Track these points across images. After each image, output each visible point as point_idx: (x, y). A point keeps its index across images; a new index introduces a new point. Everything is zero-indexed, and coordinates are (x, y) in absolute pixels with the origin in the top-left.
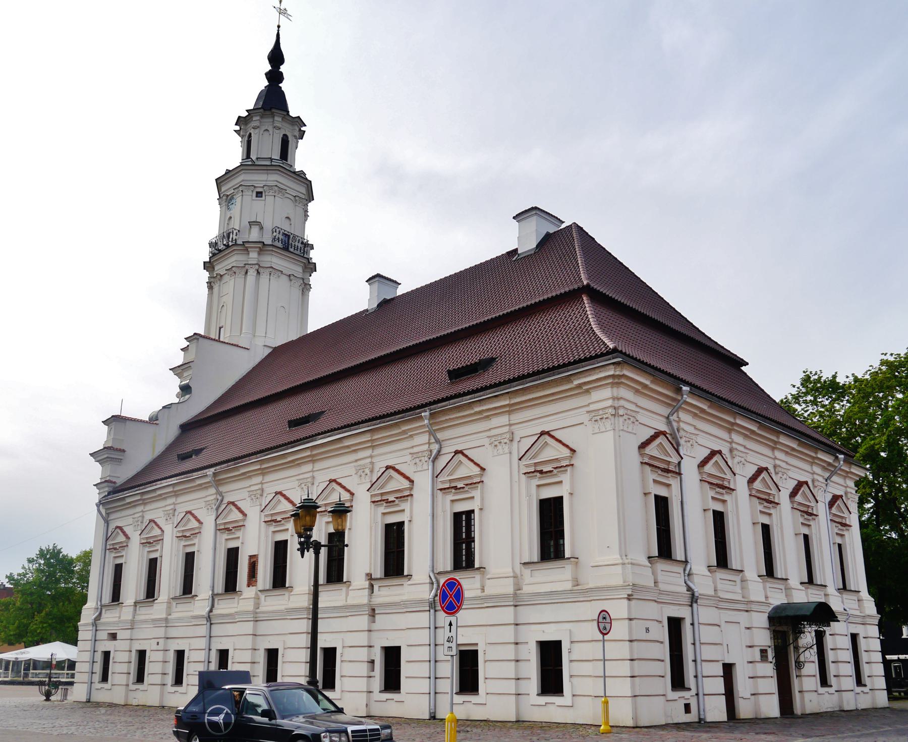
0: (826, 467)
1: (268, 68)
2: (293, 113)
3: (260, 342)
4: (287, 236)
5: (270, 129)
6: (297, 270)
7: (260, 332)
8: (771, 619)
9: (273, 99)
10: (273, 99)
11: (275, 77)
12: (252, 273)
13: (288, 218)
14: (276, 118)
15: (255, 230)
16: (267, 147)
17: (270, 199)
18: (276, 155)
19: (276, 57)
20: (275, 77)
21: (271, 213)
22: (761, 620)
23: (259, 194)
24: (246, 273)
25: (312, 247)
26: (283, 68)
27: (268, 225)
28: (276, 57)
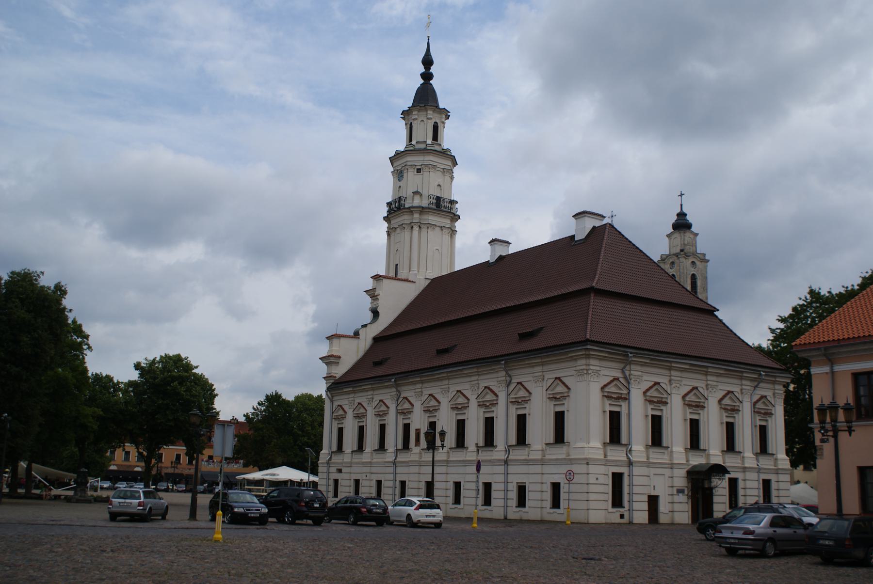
1: (424, 70)
2: (441, 107)
3: (421, 277)
4: (438, 199)
5: (425, 120)
6: (446, 222)
7: (422, 270)
9: (425, 97)
10: (425, 97)
11: (427, 76)
12: (416, 228)
13: (439, 185)
14: (429, 112)
15: (417, 198)
16: (423, 133)
19: (428, 62)
20: (427, 76)
23: (419, 171)
24: (412, 227)
25: (457, 202)
26: (433, 70)
27: (425, 193)
28: (428, 62)
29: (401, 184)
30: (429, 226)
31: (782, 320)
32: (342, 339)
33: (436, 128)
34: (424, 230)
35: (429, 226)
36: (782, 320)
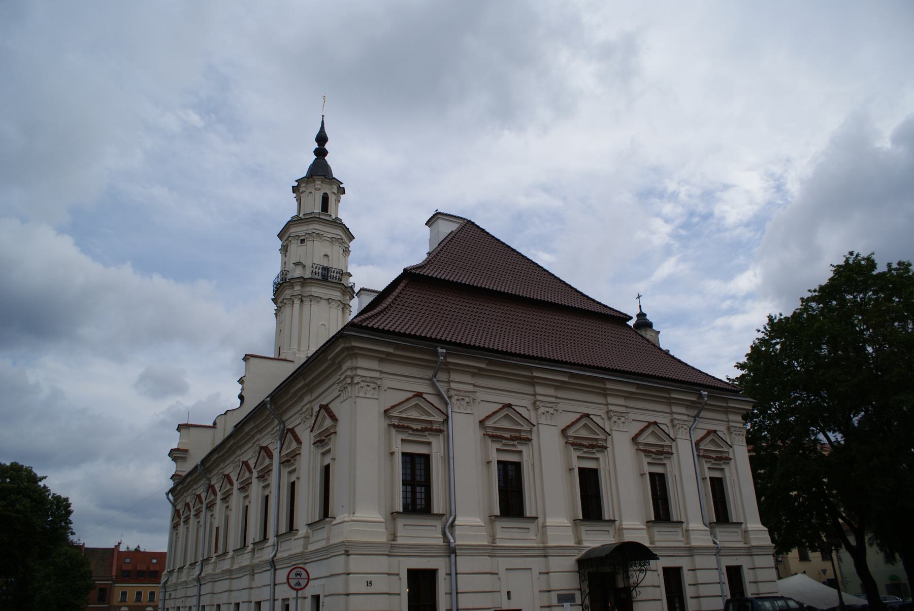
0: (690, 405)
5: (313, 191)
8: (581, 562)
11: (321, 153)
13: (326, 255)
17: (309, 244)
18: (318, 210)
19: (322, 139)
20: (321, 153)
21: (316, 253)
22: (569, 563)
23: (303, 241)
26: (327, 146)
28: (322, 139)
29: (286, 259)
30: (312, 298)
31: (741, 366)
32: (192, 429)
33: (325, 200)
34: (307, 304)
35: (312, 298)
36: (741, 366)
